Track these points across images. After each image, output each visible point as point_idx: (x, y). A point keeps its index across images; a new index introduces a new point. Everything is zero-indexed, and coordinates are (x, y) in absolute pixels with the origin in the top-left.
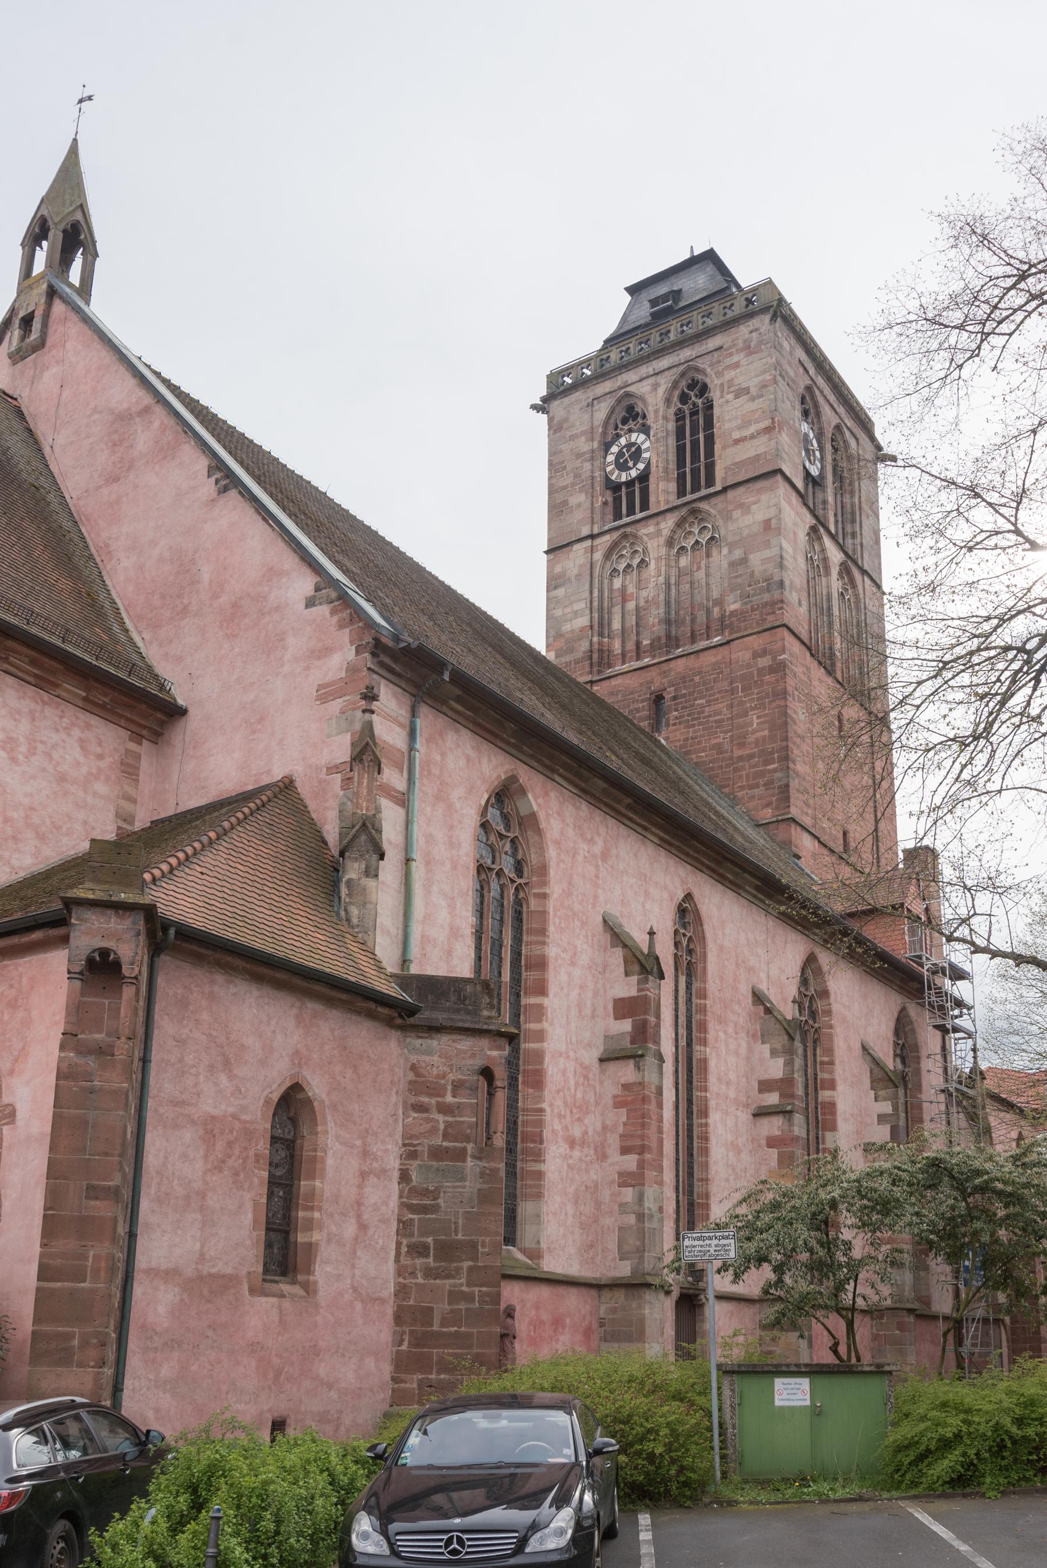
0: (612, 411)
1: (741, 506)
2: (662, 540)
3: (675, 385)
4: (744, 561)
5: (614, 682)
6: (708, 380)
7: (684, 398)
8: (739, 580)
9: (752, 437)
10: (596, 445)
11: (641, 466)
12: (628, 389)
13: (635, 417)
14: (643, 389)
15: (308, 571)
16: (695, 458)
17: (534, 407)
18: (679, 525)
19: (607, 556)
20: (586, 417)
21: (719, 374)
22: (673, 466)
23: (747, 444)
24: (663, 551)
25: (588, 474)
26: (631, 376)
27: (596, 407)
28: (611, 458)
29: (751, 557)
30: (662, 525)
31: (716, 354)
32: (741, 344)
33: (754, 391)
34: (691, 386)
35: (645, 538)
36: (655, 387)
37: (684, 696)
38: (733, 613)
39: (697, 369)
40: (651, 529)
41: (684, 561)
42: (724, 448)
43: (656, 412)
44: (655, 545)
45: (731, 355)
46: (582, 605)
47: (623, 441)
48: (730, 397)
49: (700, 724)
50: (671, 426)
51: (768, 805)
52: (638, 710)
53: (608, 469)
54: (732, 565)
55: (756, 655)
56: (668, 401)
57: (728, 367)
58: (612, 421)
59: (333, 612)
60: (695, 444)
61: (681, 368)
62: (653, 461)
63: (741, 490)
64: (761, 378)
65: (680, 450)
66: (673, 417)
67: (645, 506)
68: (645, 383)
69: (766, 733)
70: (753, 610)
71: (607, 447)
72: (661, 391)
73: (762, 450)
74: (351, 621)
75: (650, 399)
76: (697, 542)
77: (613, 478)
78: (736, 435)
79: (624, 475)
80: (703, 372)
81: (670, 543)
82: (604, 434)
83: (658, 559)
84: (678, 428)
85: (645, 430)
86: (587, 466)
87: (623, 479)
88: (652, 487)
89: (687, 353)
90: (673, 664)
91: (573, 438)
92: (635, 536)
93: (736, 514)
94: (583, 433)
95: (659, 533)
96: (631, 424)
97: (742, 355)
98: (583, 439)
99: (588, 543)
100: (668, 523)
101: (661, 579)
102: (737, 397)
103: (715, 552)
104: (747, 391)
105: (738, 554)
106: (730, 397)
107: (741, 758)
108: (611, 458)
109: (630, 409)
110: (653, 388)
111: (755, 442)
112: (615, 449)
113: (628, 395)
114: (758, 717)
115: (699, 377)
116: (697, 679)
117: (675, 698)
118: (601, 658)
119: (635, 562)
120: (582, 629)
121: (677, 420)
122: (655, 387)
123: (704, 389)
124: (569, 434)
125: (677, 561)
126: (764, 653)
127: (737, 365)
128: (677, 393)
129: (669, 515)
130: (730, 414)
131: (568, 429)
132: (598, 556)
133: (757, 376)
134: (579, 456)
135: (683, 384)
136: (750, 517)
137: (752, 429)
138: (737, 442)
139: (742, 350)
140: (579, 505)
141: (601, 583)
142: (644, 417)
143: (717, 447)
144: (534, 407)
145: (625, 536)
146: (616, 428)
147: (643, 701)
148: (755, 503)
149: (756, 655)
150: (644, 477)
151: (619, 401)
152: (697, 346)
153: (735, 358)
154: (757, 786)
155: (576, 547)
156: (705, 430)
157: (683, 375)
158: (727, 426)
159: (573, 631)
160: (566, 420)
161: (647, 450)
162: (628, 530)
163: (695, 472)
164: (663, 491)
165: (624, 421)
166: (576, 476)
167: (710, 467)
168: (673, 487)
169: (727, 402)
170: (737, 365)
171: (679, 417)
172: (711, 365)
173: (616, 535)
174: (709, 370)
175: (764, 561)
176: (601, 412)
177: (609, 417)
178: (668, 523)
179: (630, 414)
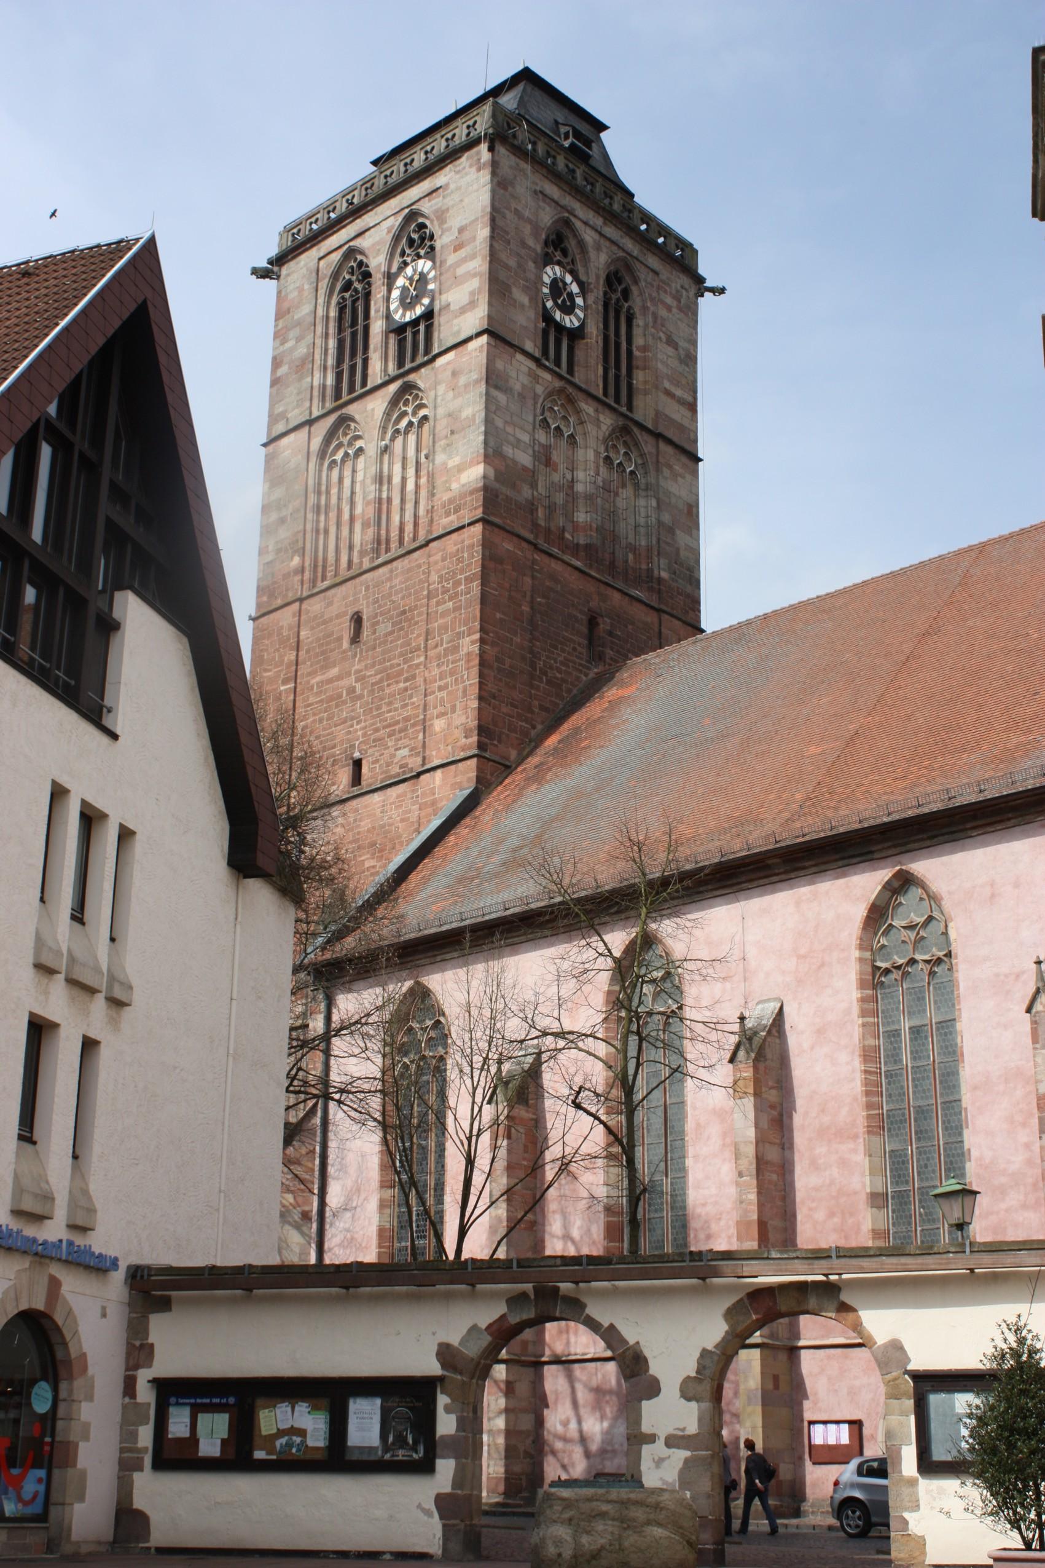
6: (634, 289)
12: (573, 219)
14: (589, 236)
36: (598, 248)
39: (629, 268)
68: (589, 231)
75: (592, 254)
80: (636, 281)
115: (628, 279)
123: (626, 294)
134: (523, 244)
138: (668, 393)
153: (669, 300)
160: (512, 184)
169: (660, 338)
170: (669, 309)
176: (547, 217)
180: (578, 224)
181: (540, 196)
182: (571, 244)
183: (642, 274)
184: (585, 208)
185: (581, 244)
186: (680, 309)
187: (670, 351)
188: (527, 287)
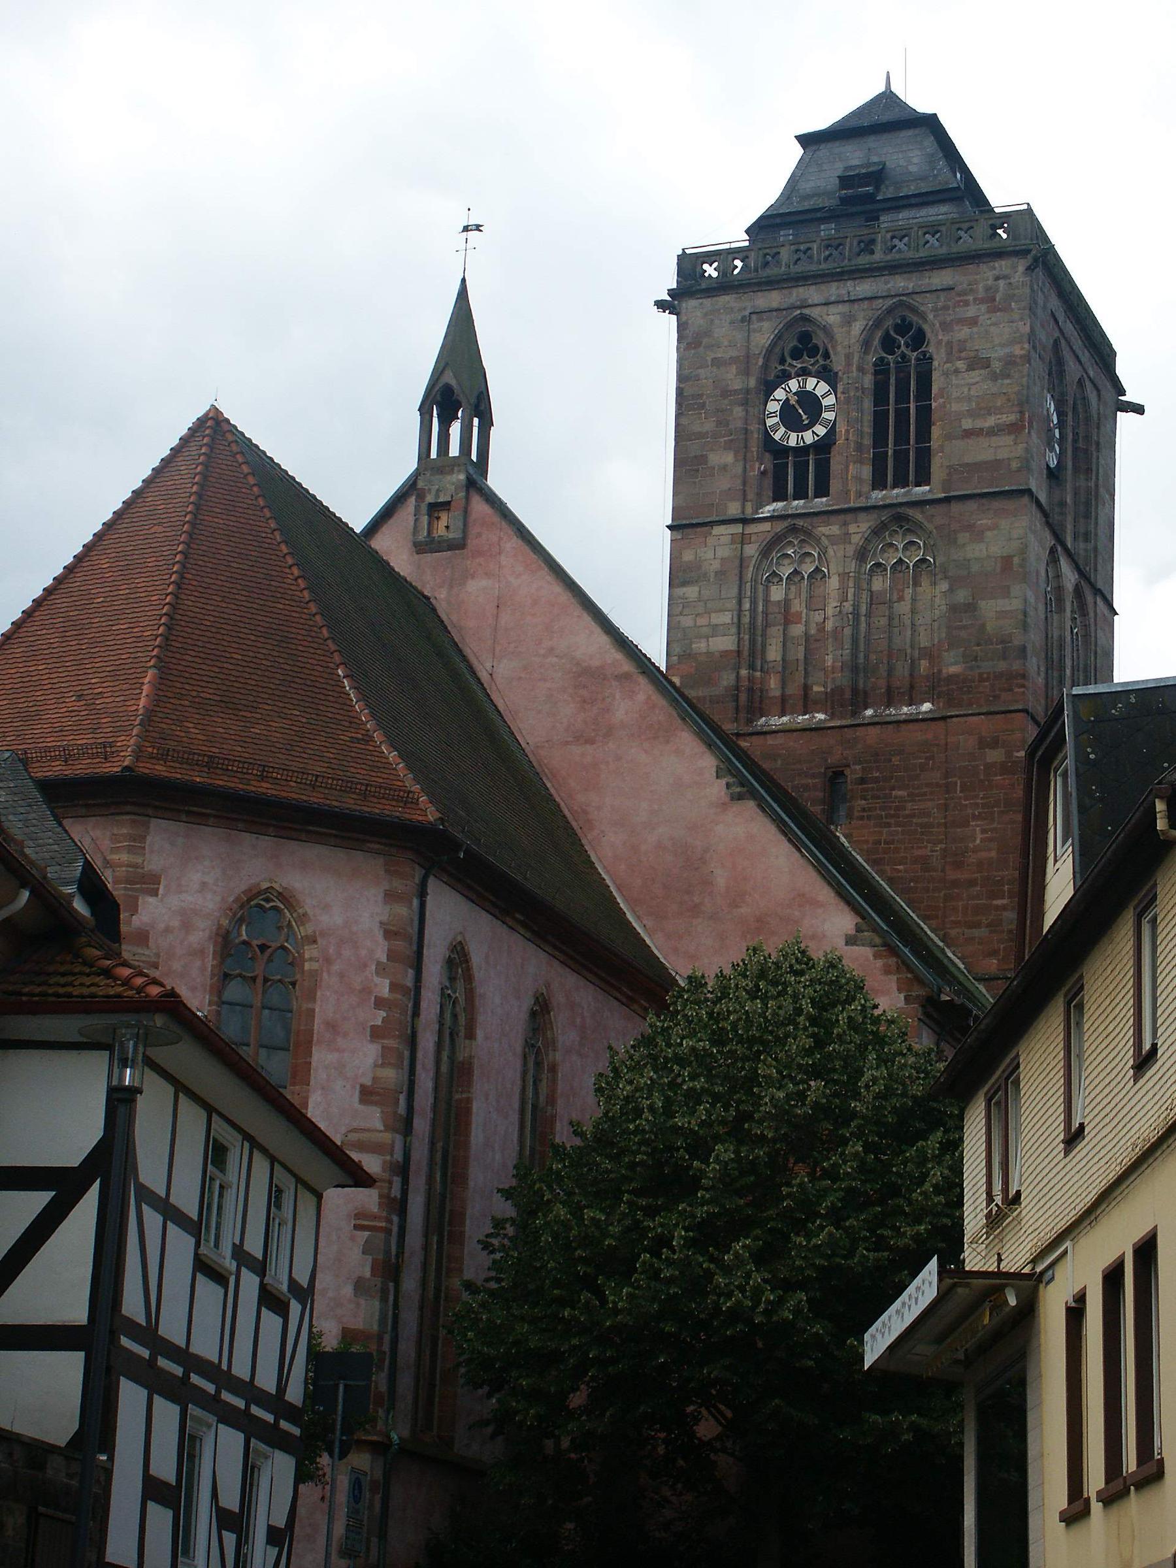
0: (779, 337)
1: (970, 527)
2: (851, 550)
3: (878, 323)
4: (970, 608)
5: (770, 741)
6: (925, 327)
7: (888, 344)
8: (963, 634)
9: (992, 432)
10: (752, 383)
11: (821, 430)
12: (806, 311)
13: (813, 352)
14: (832, 317)
15: (846, 909)
16: (902, 436)
17: (661, 305)
18: (877, 532)
19: (765, 553)
20: (739, 336)
21: (946, 327)
22: (868, 441)
23: (984, 442)
24: (852, 566)
25: (739, 424)
26: (813, 294)
27: (755, 326)
28: (773, 407)
29: (982, 604)
30: (852, 528)
31: (942, 295)
32: (981, 294)
33: (996, 366)
34: (903, 328)
35: (825, 541)
36: (849, 320)
37: (876, 780)
38: (951, 679)
39: (914, 310)
40: (835, 530)
41: (878, 584)
42: (949, 437)
43: (848, 357)
44: (840, 554)
45: (967, 304)
46: (726, 618)
47: (793, 384)
48: (960, 365)
49: (898, 825)
50: (868, 381)
51: (994, 953)
52: (806, 787)
53: (770, 422)
54: (954, 609)
55: (983, 744)
56: (866, 344)
57: (962, 321)
58: (777, 350)
59: (876, 956)
60: (903, 415)
61: (889, 302)
62: (841, 428)
63: (972, 505)
64: (1007, 350)
65: (880, 420)
66: (870, 368)
67: (822, 489)
68: (833, 309)
69: (993, 854)
70: (981, 680)
71: (768, 388)
72: (857, 327)
73: (1003, 454)
74: (898, 970)
75: (839, 333)
76: (900, 561)
77: (777, 437)
78: (967, 424)
79: (793, 436)
80: (923, 316)
81: (861, 555)
82: (766, 366)
83: (844, 576)
84: (876, 383)
85: (827, 375)
86: (738, 411)
87: (792, 443)
88: (836, 465)
89: (900, 283)
90: (860, 732)
91: (717, 362)
92: (808, 533)
93: (963, 537)
94: (733, 360)
95: (846, 538)
96: (807, 362)
97: (983, 307)
98: (734, 369)
99: (737, 529)
100: (860, 528)
101: (848, 607)
102: (971, 368)
103: (925, 582)
104: (986, 363)
105: (962, 596)
106: (960, 365)
107: (955, 883)
108: (773, 407)
109: (805, 338)
110: (844, 318)
111: (995, 441)
112: (780, 394)
113: (805, 319)
114: (983, 831)
115: (915, 319)
116: (896, 760)
117: (862, 781)
118: (751, 700)
119: (808, 568)
120: (725, 654)
121: (876, 373)
122: (849, 320)
123: (919, 339)
124: (710, 356)
125: (870, 582)
126: (994, 743)
127: (973, 322)
128: (879, 334)
129: (862, 516)
130: (957, 391)
131: (709, 347)
132: (751, 550)
133: (1003, 345)
134: (726, 393)
135: (889, 323)
136: (983, 546)
137: (991, 421)
138: (968, 434)
139: (982, 301)
140: (724, 468)
141: (754, 590)
142: (827, 356)
143: (936, 431)
144: (661, 305)
145: (793, 530)
146: (782, 361)
147: (813, 776)
148: (989, 529)
149: (983, 744)
150: (824, 446)
151: (789, 325)
152: (914, 276)
153: (971, 312)
154: (977, 925)
155: (717, 530)
156: (917, 400)
157: (890, 311)
158: (955, 407)
159: (709, 654)
160: (708, 333)
161: (829, 408)
162: (800, 522)
163: (901, 458)
164: (851, 473)
165: (796, 354)
166: (719, 423)
167: (924, 456)
168: (867, 472)
169: (957, 371)
170: (973, 322)
171: (881, 369)
172: (935, 310)
173: (780, 526)
174: (931, 316)
175: (1002, 615)
176: (764, 335)
177: (774, 344)
178: (860, 528)
179: (803, 346)
180: (814, 313)
181: (754, 317)
182: (819, 339)
183: (927, 305)
184: (823, 287)
185: (826, 330)
186: (993, 310)
187: (975, 376)
188: (732, 441)
